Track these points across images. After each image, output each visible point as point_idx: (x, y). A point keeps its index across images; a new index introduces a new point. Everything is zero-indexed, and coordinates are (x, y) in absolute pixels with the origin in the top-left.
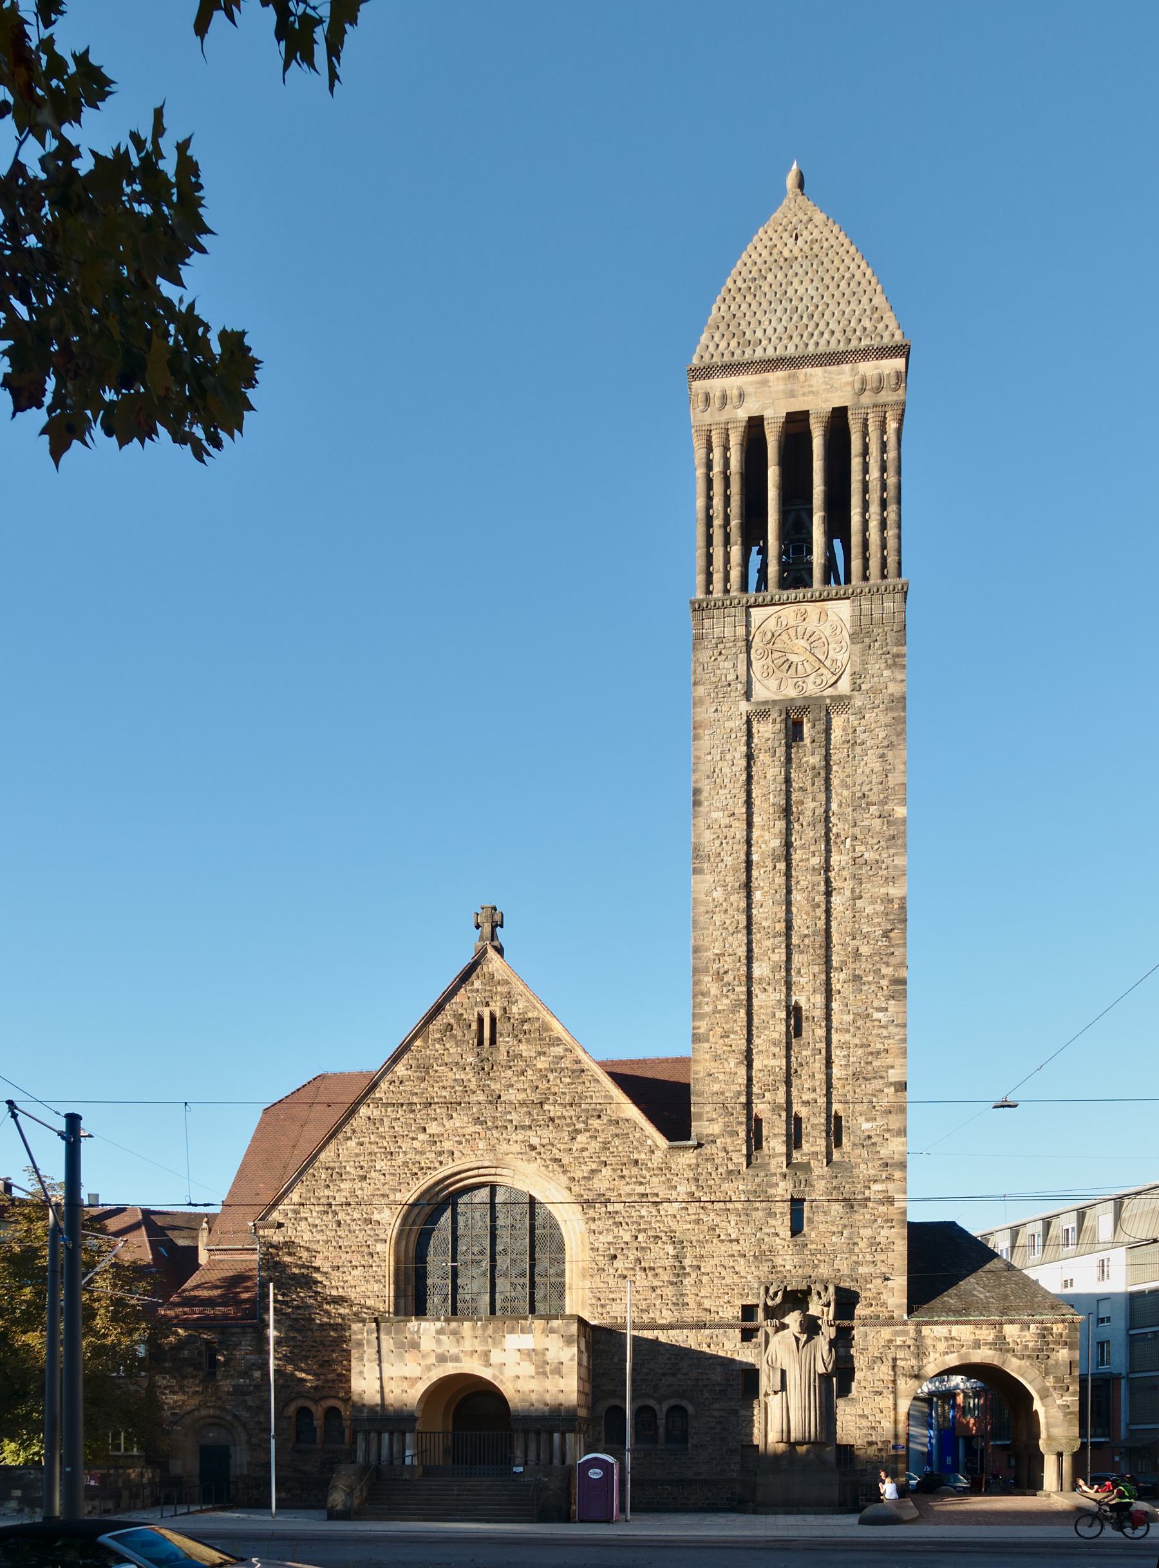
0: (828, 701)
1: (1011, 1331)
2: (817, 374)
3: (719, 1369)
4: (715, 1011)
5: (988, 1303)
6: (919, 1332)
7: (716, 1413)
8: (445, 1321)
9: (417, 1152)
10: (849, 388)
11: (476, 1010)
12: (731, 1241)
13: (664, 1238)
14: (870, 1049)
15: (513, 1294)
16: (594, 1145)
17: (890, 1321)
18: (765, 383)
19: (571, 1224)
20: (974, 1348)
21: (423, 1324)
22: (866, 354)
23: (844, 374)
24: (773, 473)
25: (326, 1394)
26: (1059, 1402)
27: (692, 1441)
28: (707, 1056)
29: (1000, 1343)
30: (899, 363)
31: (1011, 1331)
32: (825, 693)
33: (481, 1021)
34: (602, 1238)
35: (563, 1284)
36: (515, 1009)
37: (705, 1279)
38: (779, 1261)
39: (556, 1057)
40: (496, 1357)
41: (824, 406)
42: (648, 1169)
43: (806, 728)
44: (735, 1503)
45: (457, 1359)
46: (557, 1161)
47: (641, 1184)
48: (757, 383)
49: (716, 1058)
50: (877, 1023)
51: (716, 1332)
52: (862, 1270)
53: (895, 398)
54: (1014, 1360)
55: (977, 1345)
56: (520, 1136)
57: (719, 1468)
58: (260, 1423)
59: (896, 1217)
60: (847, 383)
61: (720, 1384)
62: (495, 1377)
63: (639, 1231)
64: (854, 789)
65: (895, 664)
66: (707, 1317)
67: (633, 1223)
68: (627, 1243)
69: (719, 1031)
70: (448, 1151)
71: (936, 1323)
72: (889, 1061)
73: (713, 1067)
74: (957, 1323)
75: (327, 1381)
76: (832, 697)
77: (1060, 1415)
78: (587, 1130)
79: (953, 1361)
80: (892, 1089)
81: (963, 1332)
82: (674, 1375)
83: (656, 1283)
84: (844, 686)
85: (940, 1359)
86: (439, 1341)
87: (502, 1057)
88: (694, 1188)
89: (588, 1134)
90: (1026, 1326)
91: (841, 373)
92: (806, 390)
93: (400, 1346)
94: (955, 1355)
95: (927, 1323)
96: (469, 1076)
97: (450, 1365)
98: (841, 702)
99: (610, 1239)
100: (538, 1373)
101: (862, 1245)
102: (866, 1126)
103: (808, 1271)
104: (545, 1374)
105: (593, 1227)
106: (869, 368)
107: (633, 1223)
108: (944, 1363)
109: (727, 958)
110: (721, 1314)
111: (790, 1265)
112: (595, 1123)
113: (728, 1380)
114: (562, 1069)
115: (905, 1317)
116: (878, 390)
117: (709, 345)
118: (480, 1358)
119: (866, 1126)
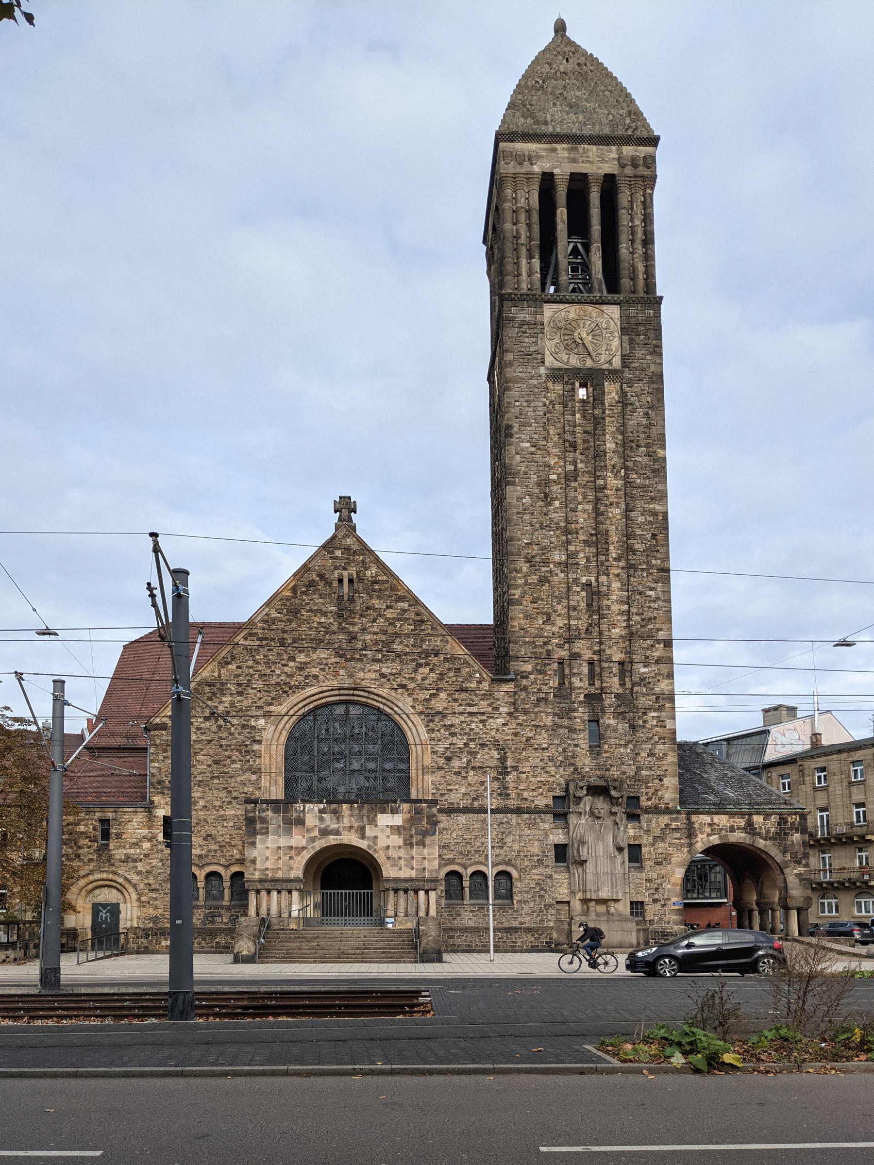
0: (606, 373)
1: (758, 820)
2: (593, 150)
3: (536, 843)
4: (526, 584)
5: (738, 799)
6: (689, 819)
7: (535, 877)
10: (616, 162)
12: (543, 749)
16: (433, 676)
17: (667, 811)
18: (554, 150)
19: (416, 731)
23: (612, 152)
24: (562, 214)
26: (795, 871)
27: (516, 898)
28: (521, 615)
29: (750, 828)
31: (758, 820)
42: (476, 695)
44: (553, 946)
47: (470, 705)
49: (526, 617)
50: (648, 599)
52: (644, 773)
54: (761, 841)
55: (732, 829)
56: (376, 667)
57: (538, 919)
60: (614, 159)
61: (537, 855)
63: (471, 740)
68: (460, 748)
71: (702, 813)
72: (658, 626)
73: (524, 623)
74: (718, 813)
76: (608, 370)
77: (797, 881)
80: (662, 645)
81: (722, 820)
82: (501, 848)
84: (617, 362)
85: (705, 839)
88: (513, 710)
90: (767, 816)
91: (611, 152)
92: (585, 159)
94: (717, 836)
98: (614, 374)
101: (644, 754)
102: (643, 670)
108: (709, 841)
110: (536, 802)
113: (544, 852)
115: (679, 808)
119: (643, 670)
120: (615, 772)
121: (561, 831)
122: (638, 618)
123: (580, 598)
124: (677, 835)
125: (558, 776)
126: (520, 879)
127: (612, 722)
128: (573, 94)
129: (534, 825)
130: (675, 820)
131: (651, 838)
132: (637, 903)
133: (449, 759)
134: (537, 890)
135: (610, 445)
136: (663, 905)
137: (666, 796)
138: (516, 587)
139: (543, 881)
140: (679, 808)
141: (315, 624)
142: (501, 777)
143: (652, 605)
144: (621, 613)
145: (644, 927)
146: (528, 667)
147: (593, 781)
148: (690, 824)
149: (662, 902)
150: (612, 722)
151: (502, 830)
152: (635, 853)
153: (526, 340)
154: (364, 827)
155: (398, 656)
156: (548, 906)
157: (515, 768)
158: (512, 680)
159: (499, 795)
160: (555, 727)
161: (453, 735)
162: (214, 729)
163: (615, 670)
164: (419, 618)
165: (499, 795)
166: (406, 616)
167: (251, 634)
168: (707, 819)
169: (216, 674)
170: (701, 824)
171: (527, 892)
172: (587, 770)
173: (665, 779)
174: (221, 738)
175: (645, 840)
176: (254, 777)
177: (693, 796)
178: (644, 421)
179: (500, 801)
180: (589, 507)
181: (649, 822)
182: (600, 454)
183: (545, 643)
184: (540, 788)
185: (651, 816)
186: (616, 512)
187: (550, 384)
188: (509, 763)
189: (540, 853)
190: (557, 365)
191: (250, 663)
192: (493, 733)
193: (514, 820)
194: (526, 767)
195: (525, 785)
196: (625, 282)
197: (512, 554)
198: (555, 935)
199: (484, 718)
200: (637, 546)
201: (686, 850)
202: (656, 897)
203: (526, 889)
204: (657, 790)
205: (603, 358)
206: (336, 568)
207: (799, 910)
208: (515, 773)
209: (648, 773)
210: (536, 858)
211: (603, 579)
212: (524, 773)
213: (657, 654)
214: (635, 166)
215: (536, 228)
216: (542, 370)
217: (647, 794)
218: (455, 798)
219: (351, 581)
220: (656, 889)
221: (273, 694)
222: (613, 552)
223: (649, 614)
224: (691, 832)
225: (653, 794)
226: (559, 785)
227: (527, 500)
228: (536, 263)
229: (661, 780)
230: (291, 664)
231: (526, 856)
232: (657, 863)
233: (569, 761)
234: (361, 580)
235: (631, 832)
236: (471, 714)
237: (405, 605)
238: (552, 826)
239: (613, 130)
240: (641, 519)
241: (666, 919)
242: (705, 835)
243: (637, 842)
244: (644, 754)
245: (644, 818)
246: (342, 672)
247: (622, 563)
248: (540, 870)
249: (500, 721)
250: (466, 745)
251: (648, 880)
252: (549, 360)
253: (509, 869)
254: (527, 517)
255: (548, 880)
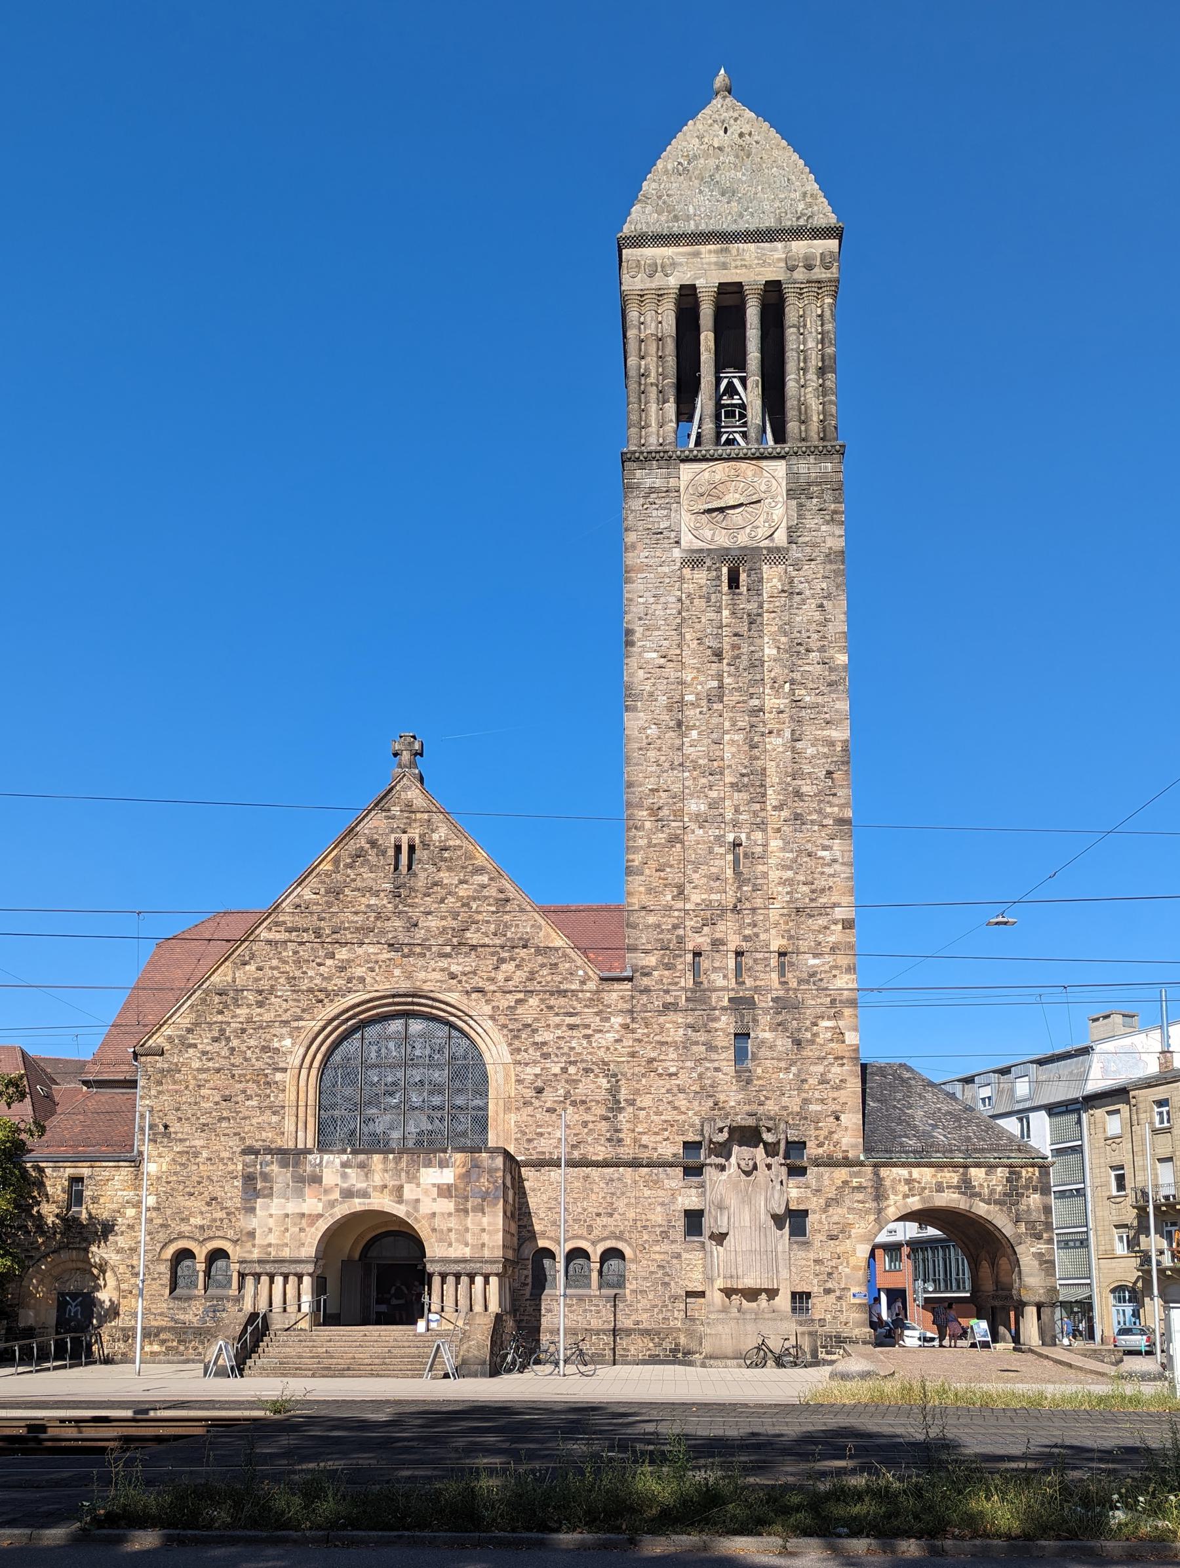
0: (765, 552)
2: (751, 249)
3: (659, 1209)
5: (950, 1145)
6: (877, 1174)
7: (657, 1256)
8: (352, 1153)
9: (324, 979)
10: (783, 264)
11: (393, 837)
12: (670, 1075)
13: (597, 1071)
14: (813, 887)
15: (430, 1128)
16: (520, 975)
17: (847, 1163)
18: (697, 254)
19: (495, 1051)
20: (937, 1191)
21: (326, 1157)
22: (797, 233)
24: (707, 339)
25: (212, 1235)
26: (1033, 1250)
27: (630, 1286)
28: (642, 889)
29: (966, 1187)
30: (833, 244)
32: (762, 545)
33: (398, 848)
34: (528, 1070)
35: (486, 1118)
36: (435, 836)
37: (642, 1114)
38: (722, 1097)
39: (479, 885)
40: (409, 1192)
41: (757, 278)
42: (579, 1000)
43: (743, 577)
45: (364, 1194)
46: (480, 991)
47: (571, 1015)
48: (689, 254)
49: (650, 891)
50: (821, 861)
51: (655, 1170)
52: (813, 1107)
53: (829, 275)
54: (982, 1204)
55: (940, 1188)
57: (661, 1316)
58: (133, 1267)
59: (847, 1054)
60: (779, 260)
61: (660, 1226)
62: (408, 1213)
63: (570, 1063)
64: (793, 636)
65: (832, 520)
66: (644, 1155)
67: (563, 1054)
68: (555, 1075)
69: (654, 865)
70: (359, 977)
71: (895, 1165)
72: (834, 899)
74: (918, 1165)
75: (215, 1220)
76: (768, 549)
77: (1036, 1263)
78: (513, 959)
79: (915, 1203)
80: (840, 927)
81: (925, 1175)
82: (611, 1215)
83: (589, 1118)
84: (781, 538)
85: (900, 1203)
86: (344, 1176)
87: (421, 882)
88: (629, 1021)
89: (513, 964)
91: (776, 250)
92: (739, 263)
93: (300, 1180)
94: (917, 1198)
95: (885, 1165)
96: (383, 901)
97: (357, 1200)
98: (777, 554)
99: (538, 1070)
100: (457, 1210)
101: (812, 1081)
102: (812, 962)
103: (754, 1108)
104: (466, 1211)
105: (519, 1057)
106: (800, 247)
107: (563, 1054)
108: (905, 1205)
109: (661, 794)
110: (660, 1151)
111: (735, 1102)
112: (523, 953)
113: (669, 1221)
114: (486, 898)
115: (862, 1158)
116: (809, 267)
117: (640, 218)
118: (391, 1193)
119: (812, 962)
120: (771, 1107)
121: (694, 1191)
122: (806, 889)
123: (724, 863)
124: (860, 1196)
125: (690, 1113)
126: (635, 1260)
127: (768, 1035)
128: (726, 177)
129: (656, 1182)
130: (857, 1175)
131: (822, 1201)
132: (801, 1294)
133: (540, 1091)
134: (660, 1274)
135: (770, 651)
136: (839, 1298)
137: (844, 1141)
138: (636, 850)
139: (668, 1262)
140: (862, 1158)
141: (363, 908)
142: (611, 1115)
143: (827, 870)
144: (784, 882)
145: (811, 1329)
146: (651, 960)
147: (741, 1120)
148: (878, 1182)
149: (838, 1293)
150: (768, 1035)
151: (613, 1190)
152: (794, 1221)
153: (655, 513)
154: (402, 1187)
155: (474, 948)
156: (675, 1298)
157: (632, 1103)
158: (630, 979)
159: (609, 1140)
160: (687, 1044)
161: (546, 1056)
162: (225, 1052)
163: (774, 962)
164: (502, 896)
165: (609, 1140)
166: (485, 893)
167: (277, 924)
168: (903, 1172)
169: (229, 979)
170: (894, 1180)
171: (645, 1279)
172: (732, 1104)
173: (842, 1117)
174: (233, 1065)
175: (813, 1204)
176: (275, 1119)
177: (883, 1141)
178: (817, 616)
179: (610, 1149)
180: (740, 737)
181: (819, 1177)
182: (756, 664)
183: (675, 927)
184: (666, 1130)
185: (822, 1169)
186: (775, 743)
187: (687, 572)
188: (623, 1094)
189: (664, 1223)
190: (698, 544)
191: (275, 962)
192: (601, 1053)
193: (628, 1176)
194: (645, 1101)
195: (645, 1125)
196: (792, 427)
197: (629, 805)
198: (683, 1340)
199: (590, 1032)
200: (804, 789)
201: (872, 1217)
202: (829, 1285)
203: (643, 1274)
204: (831, 1133)
205: (762, 532)
206: (393, 831)
207: (1039, 1306)
208: (630, 1109)
209: (818, 1108)
210: (658, 1230)
211: (758, 836)
212: (643, 1109)
213: (832, 939)
214: (809, 267)
215: (671, 361)
216: (677, 553)
217: (817, 1137)
218: (545, 1146)
219: (412, 848)
220: (830, 1274)
221: (304, 1004)
222: (772, 798)
223: (821, 883)
224: (879, 1194)
225: (826, 1138)
226: (692, 1126)
227: (653, 731)
228: (671, 408)
229: (837, 1118)
230: (329, 962)
231: (645, 1227)
232: (832, 1238)
233: (707, 1091)
234: (426, 846)
235: (794, 1193)
236: (572, 1027)
237: (484, 879)
238: (681, 1184)
239: (780, 220)
240: (811, 751)
241: (843, 1318)
242: (900, 1197)
243: (802, 1207)
244: (812, 1081)
245: (812, 1171)
246: (397, 972)
247: (785, 814)
248: (665, 1247)
249: (611, 1037)
250: (564, 1070)
251: (817, 1261)
252: (687, 540)
253: (620, 1245)
254: (652, 754)
255: (675, 1261)
